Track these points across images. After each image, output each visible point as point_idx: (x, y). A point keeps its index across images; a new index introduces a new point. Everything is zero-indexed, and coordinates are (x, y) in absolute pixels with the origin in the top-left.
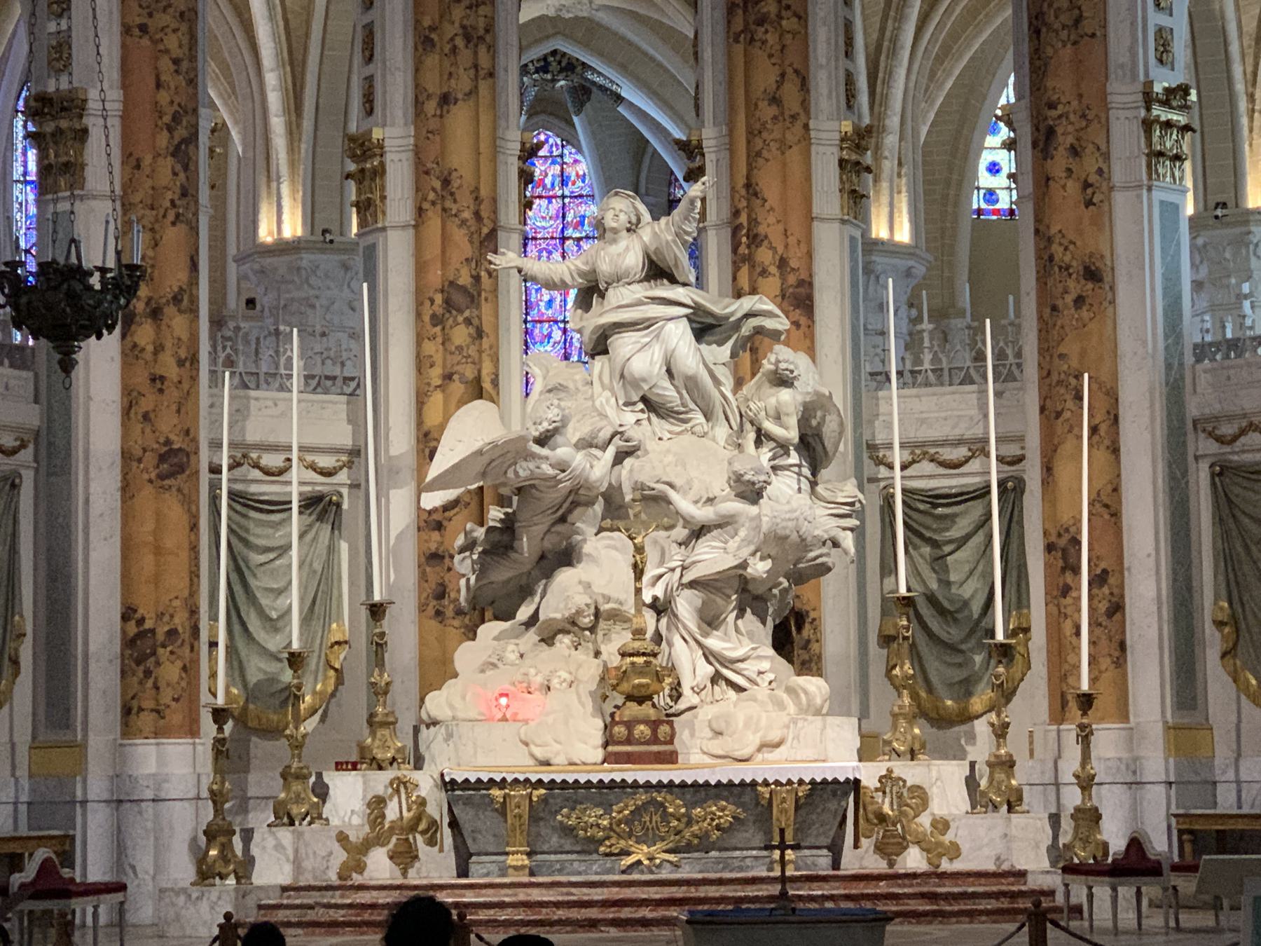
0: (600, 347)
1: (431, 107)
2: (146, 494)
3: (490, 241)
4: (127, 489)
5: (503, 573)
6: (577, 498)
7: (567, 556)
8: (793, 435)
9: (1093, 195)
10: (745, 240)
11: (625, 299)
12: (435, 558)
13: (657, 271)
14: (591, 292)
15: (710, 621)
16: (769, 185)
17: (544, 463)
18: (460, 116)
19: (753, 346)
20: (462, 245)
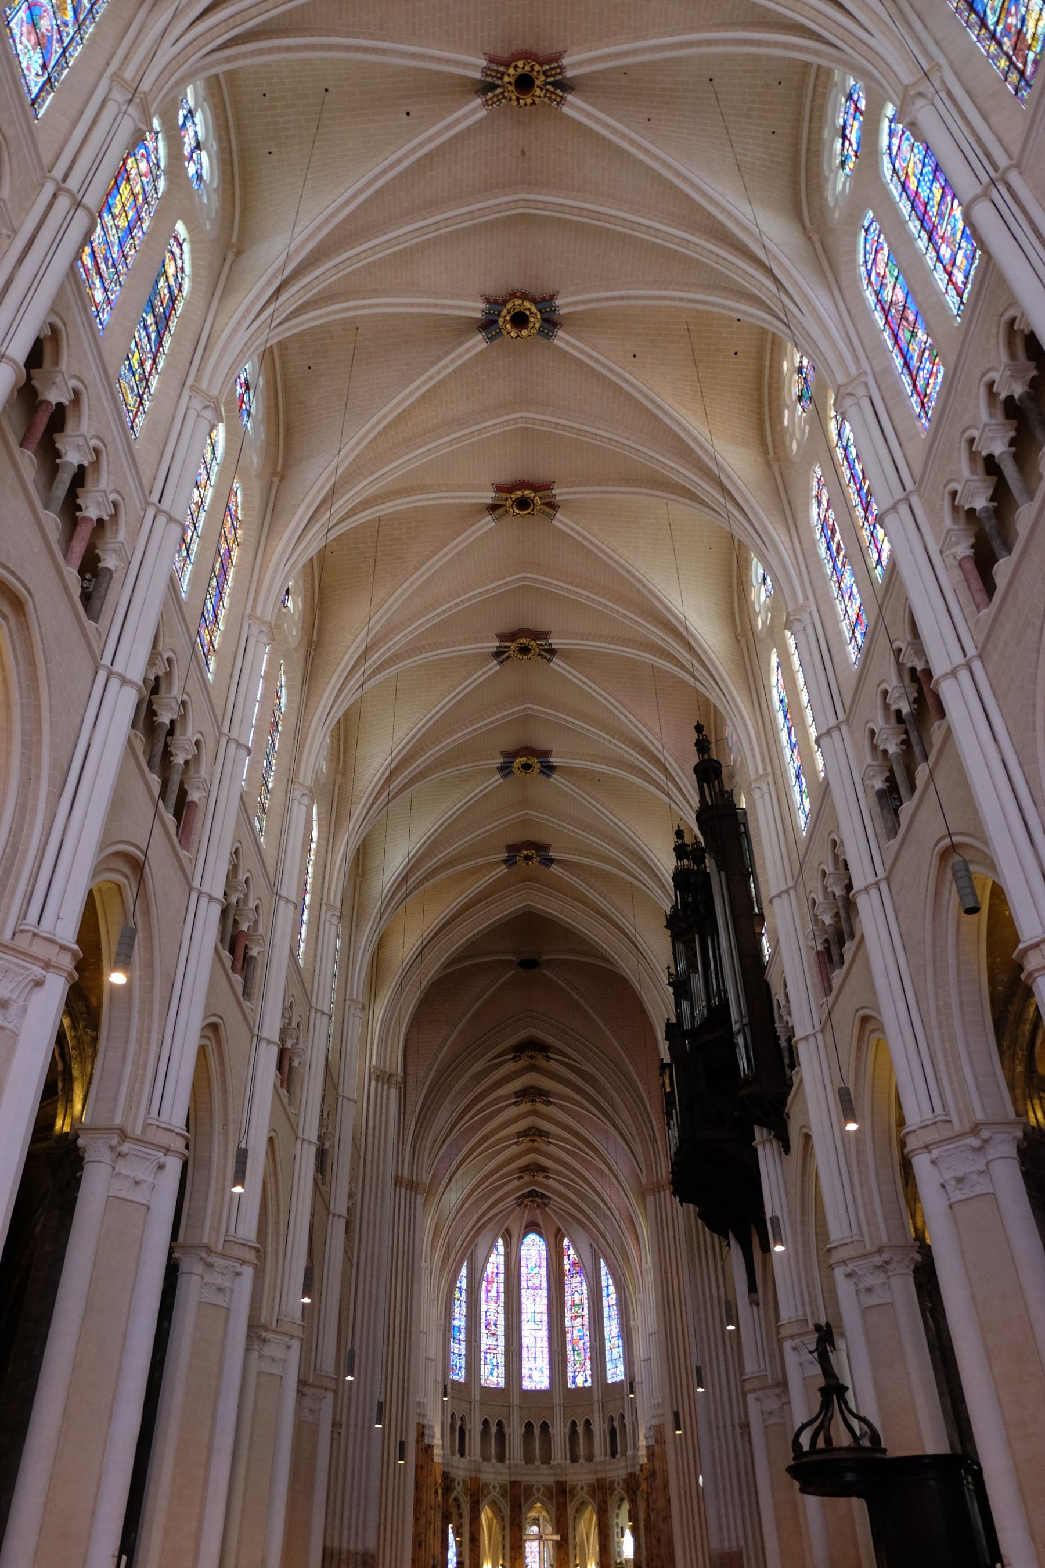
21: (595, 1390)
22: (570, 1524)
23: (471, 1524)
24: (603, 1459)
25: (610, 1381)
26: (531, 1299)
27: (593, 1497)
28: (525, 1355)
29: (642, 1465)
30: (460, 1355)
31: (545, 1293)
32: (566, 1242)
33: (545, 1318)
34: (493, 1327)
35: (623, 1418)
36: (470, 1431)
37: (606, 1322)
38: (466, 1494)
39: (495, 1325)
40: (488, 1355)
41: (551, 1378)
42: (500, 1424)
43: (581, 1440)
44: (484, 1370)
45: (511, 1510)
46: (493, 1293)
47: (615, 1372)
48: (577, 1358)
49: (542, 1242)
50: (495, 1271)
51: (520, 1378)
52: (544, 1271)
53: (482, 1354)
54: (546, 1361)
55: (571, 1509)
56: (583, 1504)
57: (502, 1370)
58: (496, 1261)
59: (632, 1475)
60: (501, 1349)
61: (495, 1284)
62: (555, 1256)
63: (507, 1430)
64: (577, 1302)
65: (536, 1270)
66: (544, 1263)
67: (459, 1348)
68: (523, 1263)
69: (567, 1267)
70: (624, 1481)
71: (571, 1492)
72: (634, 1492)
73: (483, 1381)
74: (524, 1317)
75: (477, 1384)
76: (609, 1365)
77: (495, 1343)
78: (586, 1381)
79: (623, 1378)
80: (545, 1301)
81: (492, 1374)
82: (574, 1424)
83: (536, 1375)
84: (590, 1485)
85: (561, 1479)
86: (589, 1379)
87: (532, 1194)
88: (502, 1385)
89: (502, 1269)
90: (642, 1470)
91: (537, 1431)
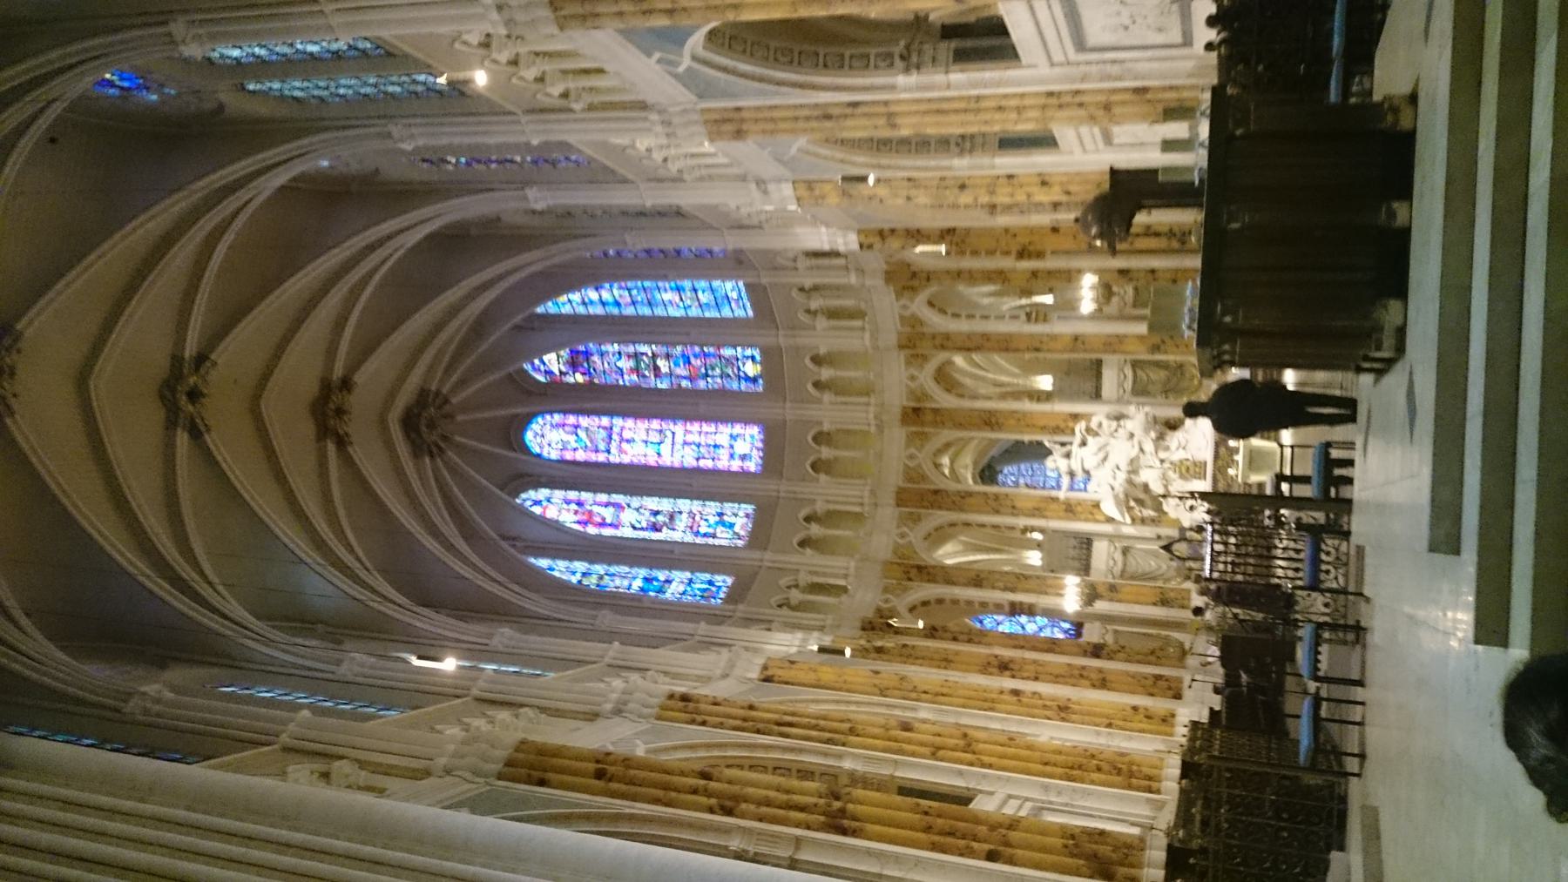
0: (1087, 473)
1: (1015, 511)
2: (1120, 596)
3: (1055, 500)
4: (1120, 601)
5: (1149, 502)
6: (1130, 482)
7: (1146, 487)
8: (1114, 424)
9: (1054, 337)
10: (1057, 430)
11: (1075, 465)
12: (1143, 521)
13: (1068, 455)
14: (1072, 474)
15: (1167, 449)
16: (1042, 423)
17: (1119, 489)
18: (1018, 504)
19: (1088, 430)
20: (1054, 506)
21: (770, 341)
22: (967, 404)
23: (954, 584)
24: (867, 335)
25: (751, 313)
26: (625, 445)
27: (925, 358)
28: (706, 464)
29: (861, 246)
30: (691, 581)
31: (618, 422)
32: (541, 378)
33: (655, 424)
34: (660, 518)
35: (802, 289)
36: (811, 573)
37: (659, 311)
38: (905, 589)
39: (656, 513)
40: (703, 530)
41: (746, 422)
42: (808, 519)
43: (840, 373)
44: (724, 538)
45: (940, 508)
46: (608, 514)
47: (729, 297)
48: (718, 371)
49: (540, 419)
50: (574, 507)
51: (744, 473)
52: (584, 421)
53: (699, 540)
54: (721, 427)
55: (946, 401)
56: (944, 377)
57: (729, 507)
58: (555, 506)
59: (889, 277)
60: (696, 506)
61: (596, 509)
62: (559, 397)
63: (820, 507)
64: (631, 363)
65: (582, 434)
66: (571, 419)
67: (678, 585)
68: (568, 456)
69: (580, 378)
70: (899, 295)
71: (918, 400)
72: (914, 275)
73: (740, 543)
74: (652, 460)
75: (738, 554)
76: (726, 312)
77: (685, 516)
78: (753, 358)
79: (741, 284)
80: (630, 423)
81: (732, 526)
82: (817, 385)
83: (737, 446)
84: (908, 363)
85: (899, 417)
86: (749, 352)
87: (410, 422)
88: (750, 508)
89: (573, 495)
90: (870, 247)
91: (826, 452)
